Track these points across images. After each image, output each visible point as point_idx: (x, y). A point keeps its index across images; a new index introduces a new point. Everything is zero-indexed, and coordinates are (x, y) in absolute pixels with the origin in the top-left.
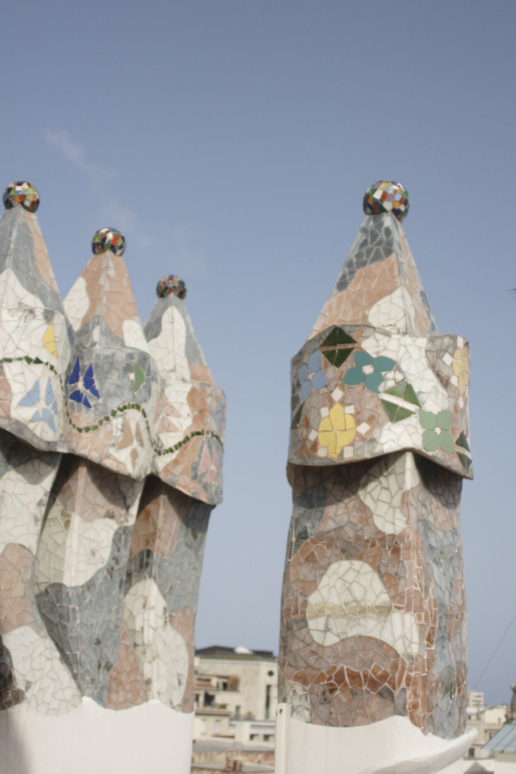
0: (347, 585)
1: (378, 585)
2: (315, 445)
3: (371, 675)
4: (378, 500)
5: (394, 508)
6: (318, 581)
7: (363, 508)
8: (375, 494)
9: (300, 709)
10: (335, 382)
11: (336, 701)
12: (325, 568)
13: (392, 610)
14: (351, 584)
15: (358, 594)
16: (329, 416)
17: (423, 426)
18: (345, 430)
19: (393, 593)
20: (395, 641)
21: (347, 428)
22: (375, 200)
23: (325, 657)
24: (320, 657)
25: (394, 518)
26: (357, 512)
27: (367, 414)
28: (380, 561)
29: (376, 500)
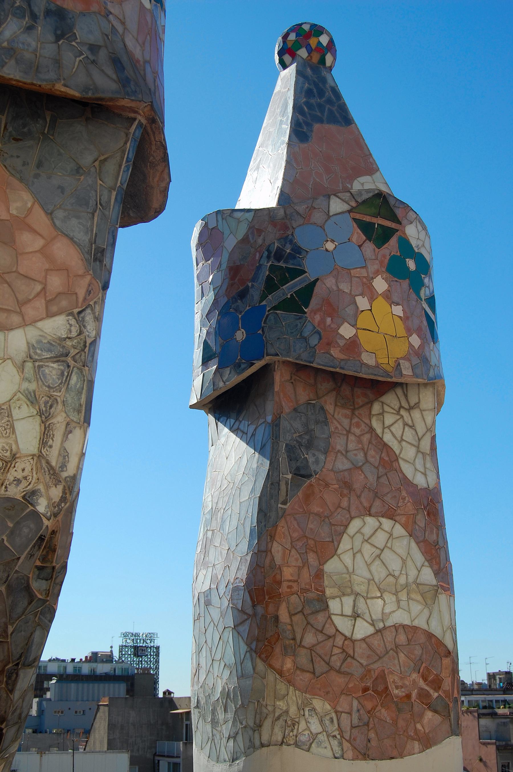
0: (378, 552)
10: (376, 267)
16: (371, 310)
24: (350, 656)
25: (425, 468)
26: (374, 451)
29: (399, 439)
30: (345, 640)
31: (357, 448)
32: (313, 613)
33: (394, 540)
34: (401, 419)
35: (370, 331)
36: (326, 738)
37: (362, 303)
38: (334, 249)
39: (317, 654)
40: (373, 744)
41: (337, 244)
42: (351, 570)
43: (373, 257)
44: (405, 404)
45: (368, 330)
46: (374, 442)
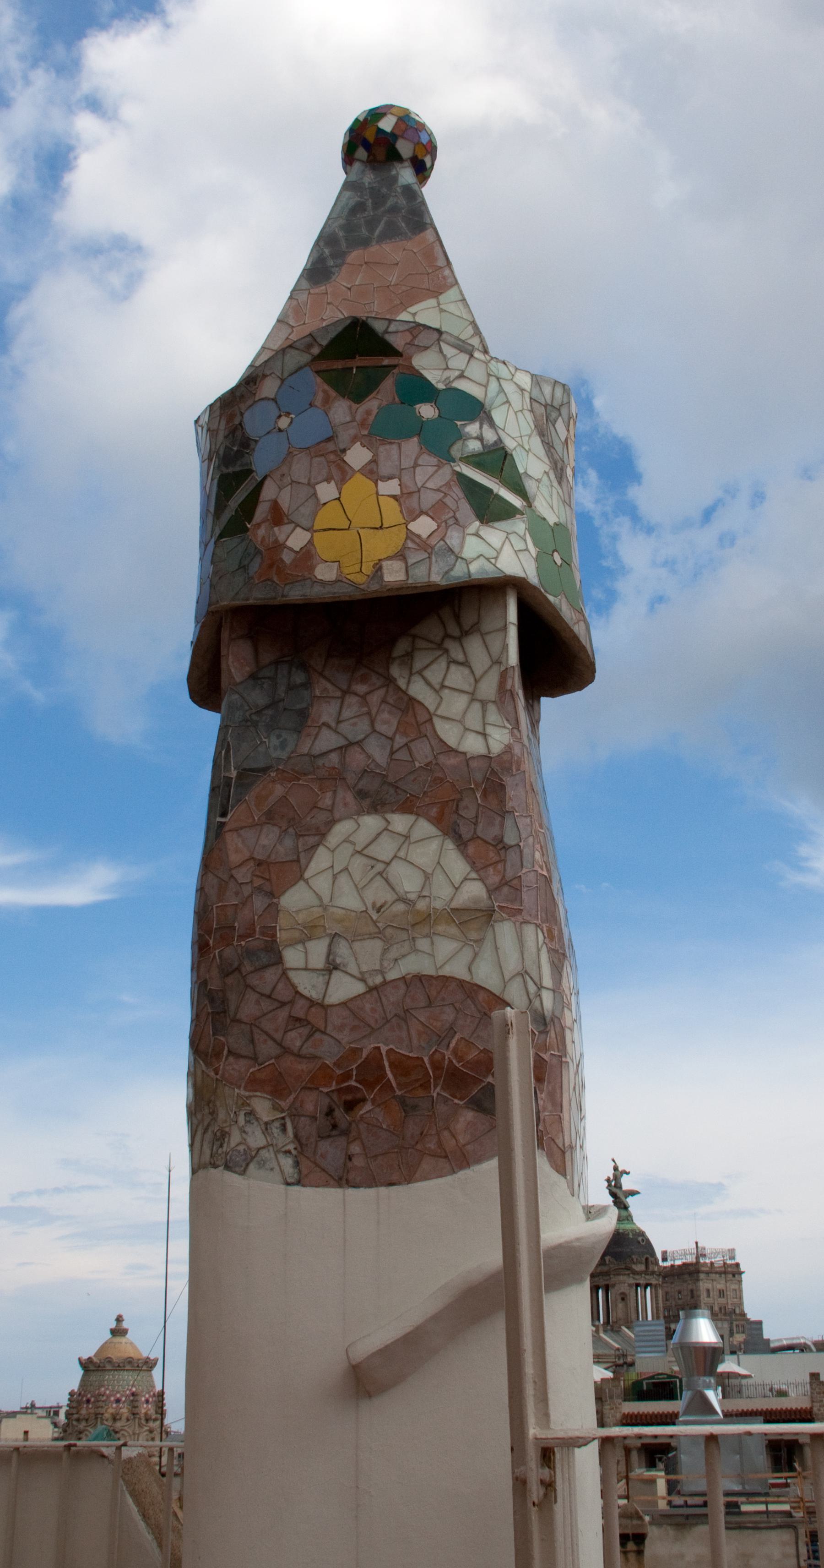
0: (380, 867)
1: (456, 865)
2: (307, 555)
3: (450, 1061)
4: (443, 686)
5: (484, 703)
6: (303, 861)
7: (409, 705)
8: (435, 674)
9: (264, 1154)
10: (352, 432)
11: (363, 1126)
12: (322, 834)
13: (496, 916)
14: (388, 864)
15: (409, 882)
16: (339, 499)
17: (535, 544)
18: (381, 527)
19: (494, 879)
20: (505, 984)
21: (385, 525)
22: (380, 131)
23: (329, 1030)
24: (318, 1030)
25: (484, 724)
26: (390, 712)
27: (429, 499)
28: (456, 811)
29: (437, 687)
30: (311, 1007)
31: (359, 713)
32: (256, 970)
33: (412, 847)
34: (445, 656)
35: (334, 529)
36: (273, 1155)
37: (326, 491)
38: (289, 425)
39: (262, 1030)
40: (356, 1163)
41: (293, 416)
42: (326, 900)
43: (348, 419)
44: (453, 630)
45: (330, 529)
46: (391, 701)
